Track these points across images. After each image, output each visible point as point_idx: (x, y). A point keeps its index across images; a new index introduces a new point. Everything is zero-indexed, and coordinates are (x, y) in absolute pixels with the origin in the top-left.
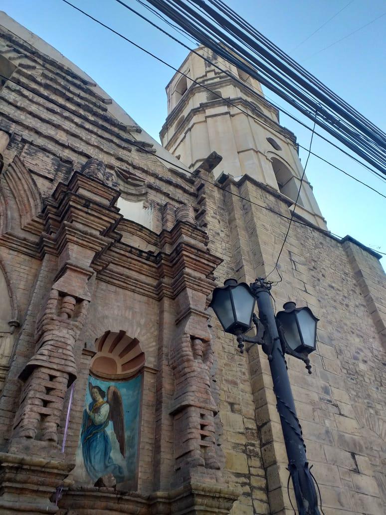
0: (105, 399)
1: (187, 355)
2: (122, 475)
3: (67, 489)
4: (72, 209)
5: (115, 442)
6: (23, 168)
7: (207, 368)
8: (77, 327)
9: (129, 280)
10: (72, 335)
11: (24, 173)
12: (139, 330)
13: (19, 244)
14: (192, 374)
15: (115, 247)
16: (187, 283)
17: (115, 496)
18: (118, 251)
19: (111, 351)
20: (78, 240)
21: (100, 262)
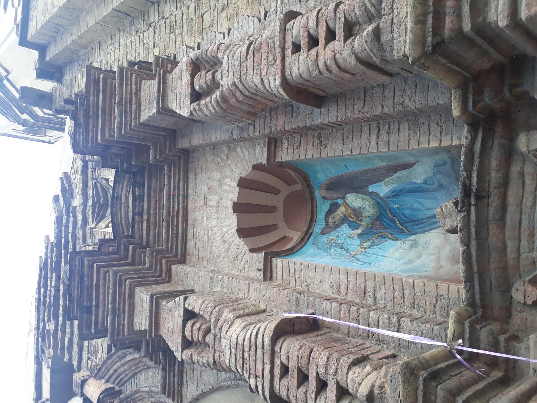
0: (340, 201)
1: (217, 102)
2: (449, 161)
3: (467, 324)
4: (100, 327)
5: (399, 178)
6: (103, 369)
7: (226, 57)
8: (217, 320)
9: (171, 210)
10: (227, 332)
11: (107, 367)
12: (227, 181)
13: (172, 374)
14: (240, 86)
15: (141, 238)
16: (133, 124)
17: (473, 209)
18: (145, 232)
19: (273, 209)
20: (126, 318)
21: (156, 266)
